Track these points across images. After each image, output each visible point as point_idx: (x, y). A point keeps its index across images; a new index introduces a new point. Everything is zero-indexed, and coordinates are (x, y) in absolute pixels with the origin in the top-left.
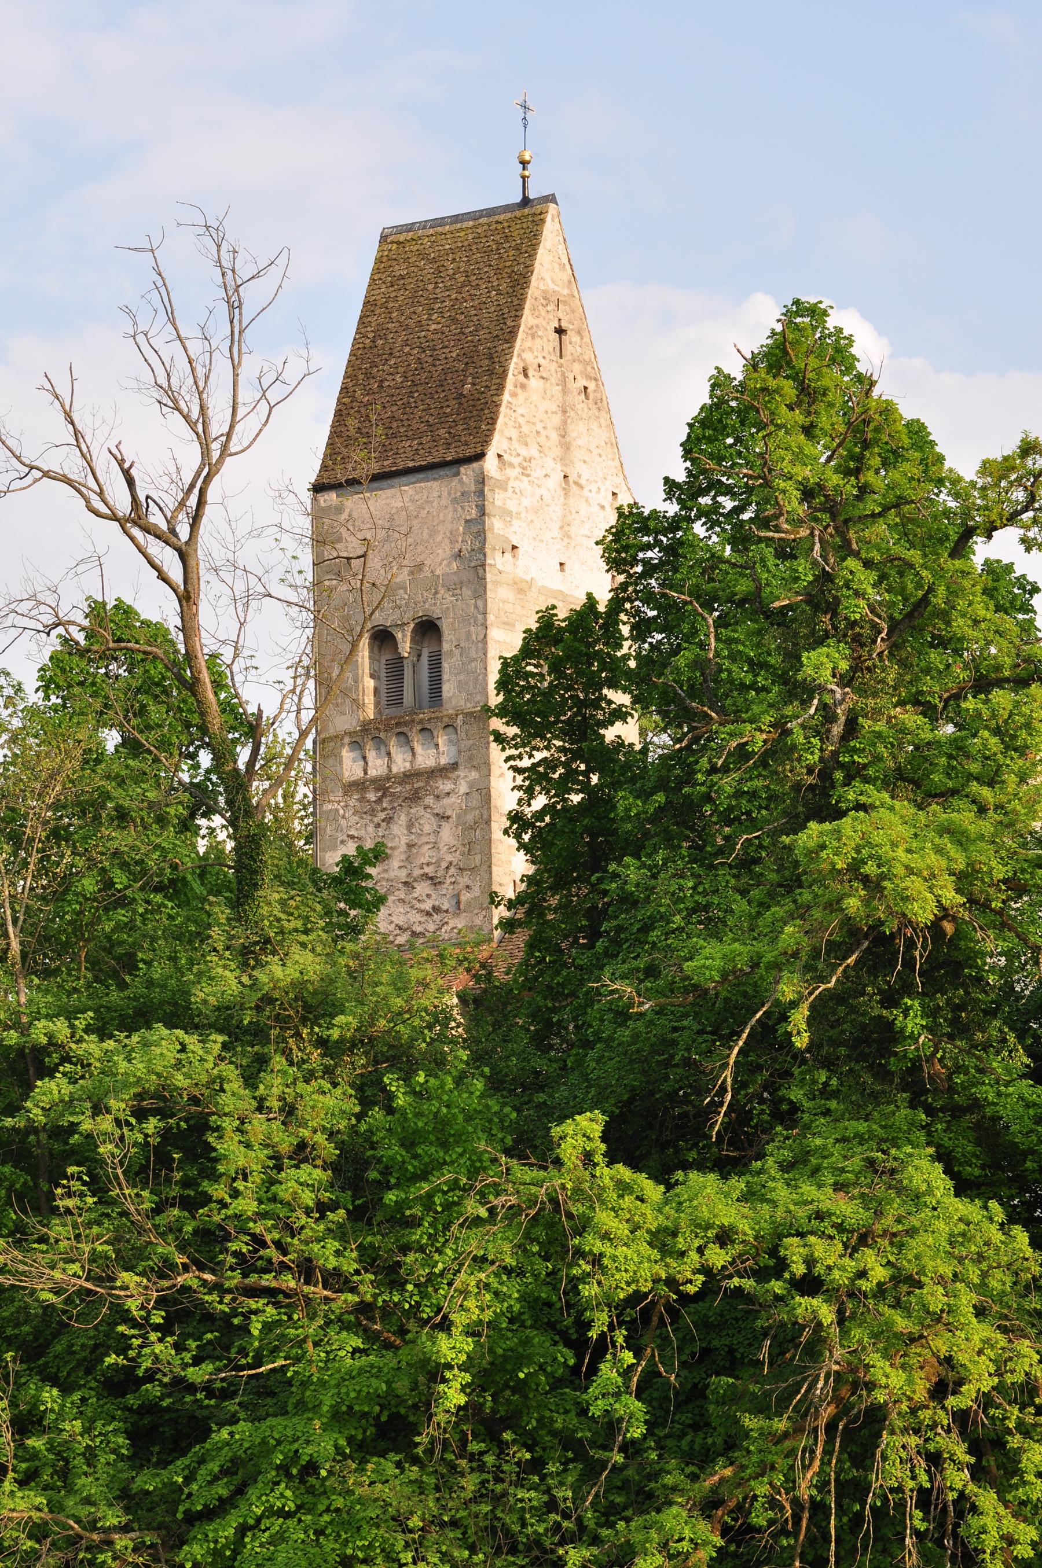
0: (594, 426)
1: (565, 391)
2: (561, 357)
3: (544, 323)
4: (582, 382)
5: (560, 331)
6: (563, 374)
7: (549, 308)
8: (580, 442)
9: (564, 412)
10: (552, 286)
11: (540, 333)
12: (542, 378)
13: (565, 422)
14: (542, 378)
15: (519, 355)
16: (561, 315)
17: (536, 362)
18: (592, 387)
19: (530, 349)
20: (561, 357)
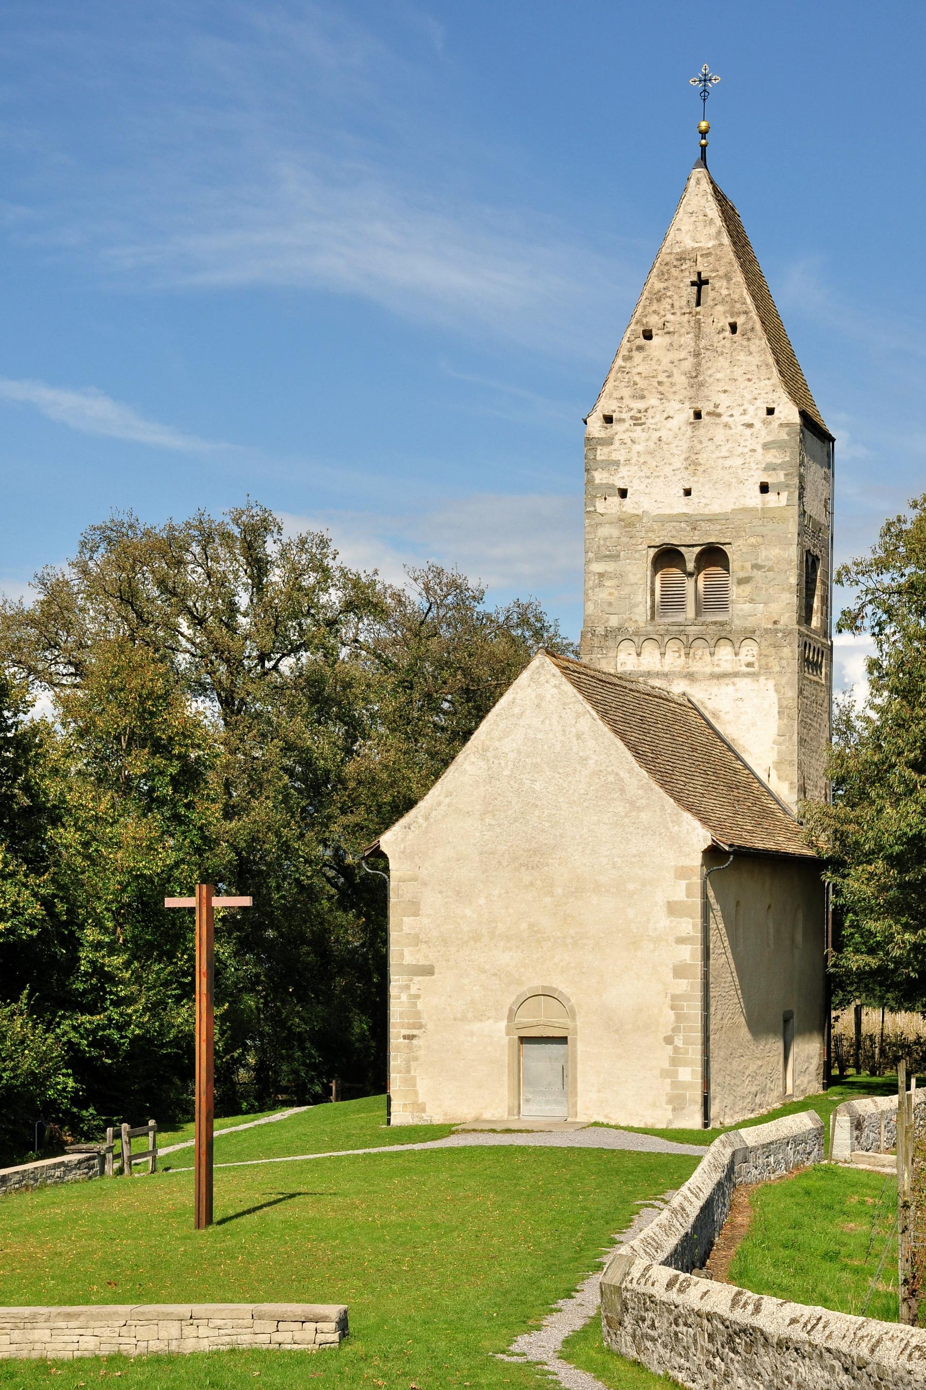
0: (742, 357)
1: (698, 337)
2: (698, 304)
3: (676, 283)
4: (725, 322)
5: (700, 283)
6: (698, 322)
7: (683, 267)
8: (719, 376)
9: (697, 355)
10: (689, 244)
11: (669, 294)
12: (669, 333)
13: (699, 364)
14: (669, 333)
15: (637, 323)
16: (700, 268)
17: (663, 320)
18: (740, 321)
19: (655, 312)
20: (698, 304)
